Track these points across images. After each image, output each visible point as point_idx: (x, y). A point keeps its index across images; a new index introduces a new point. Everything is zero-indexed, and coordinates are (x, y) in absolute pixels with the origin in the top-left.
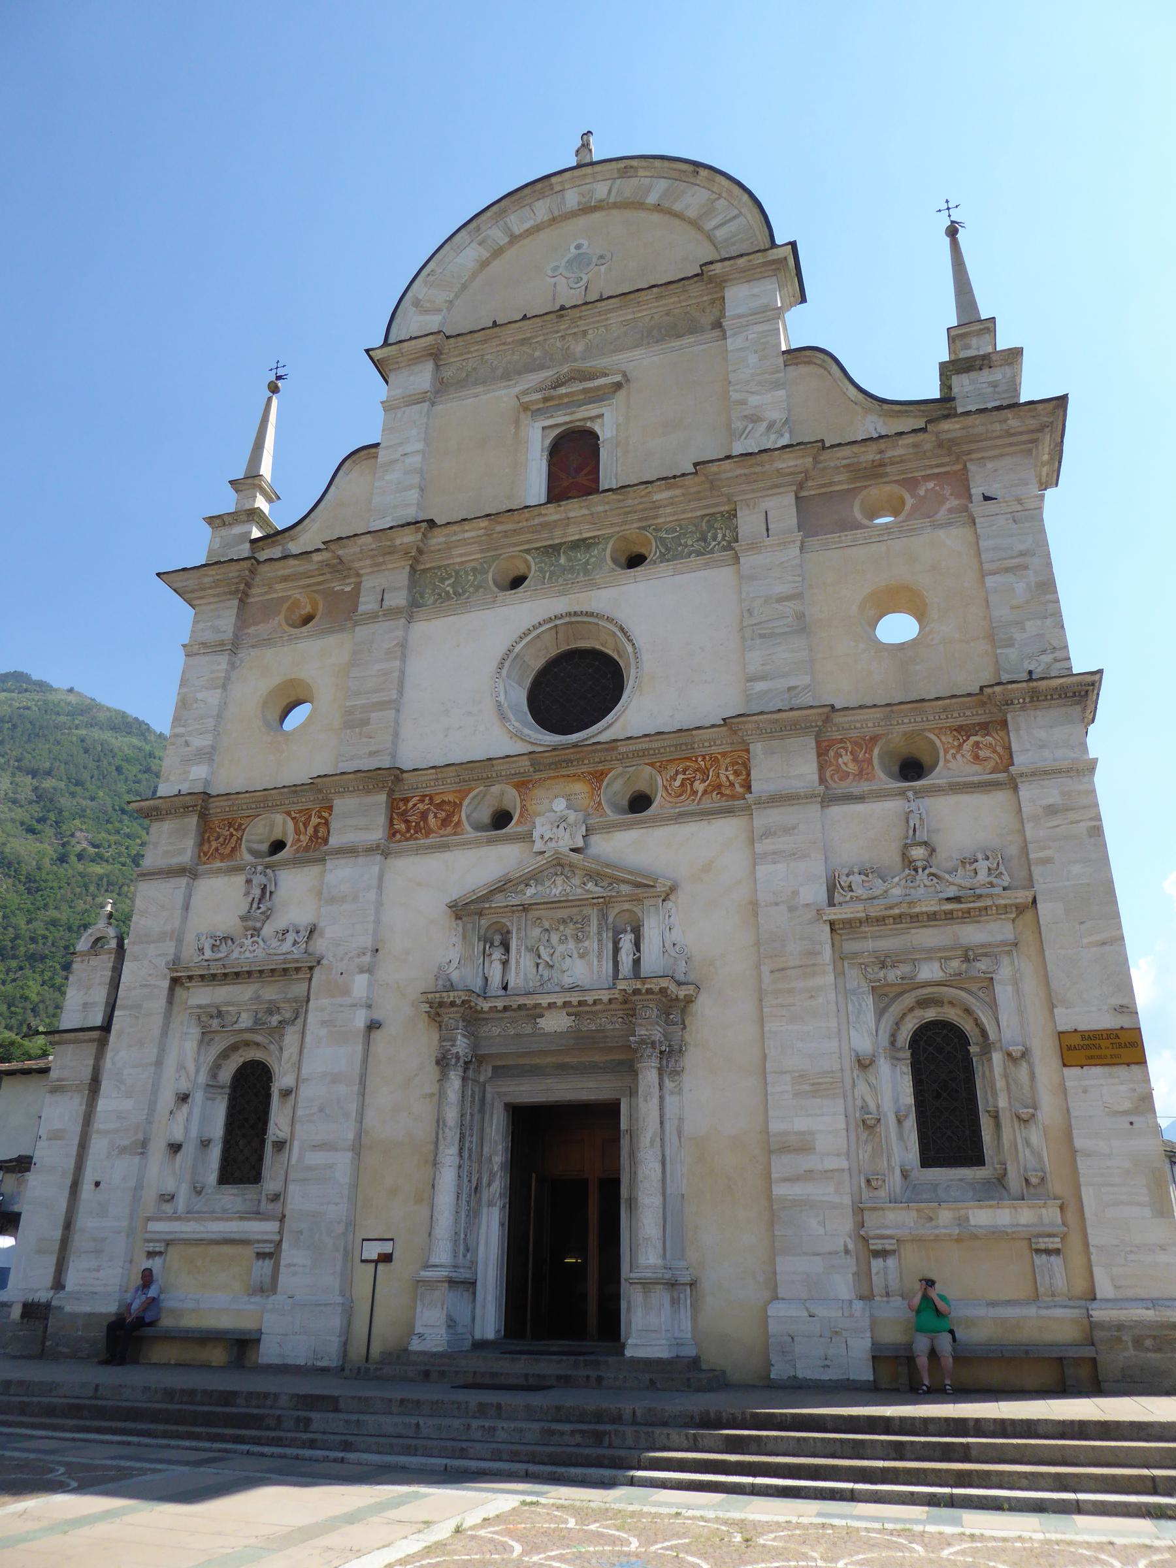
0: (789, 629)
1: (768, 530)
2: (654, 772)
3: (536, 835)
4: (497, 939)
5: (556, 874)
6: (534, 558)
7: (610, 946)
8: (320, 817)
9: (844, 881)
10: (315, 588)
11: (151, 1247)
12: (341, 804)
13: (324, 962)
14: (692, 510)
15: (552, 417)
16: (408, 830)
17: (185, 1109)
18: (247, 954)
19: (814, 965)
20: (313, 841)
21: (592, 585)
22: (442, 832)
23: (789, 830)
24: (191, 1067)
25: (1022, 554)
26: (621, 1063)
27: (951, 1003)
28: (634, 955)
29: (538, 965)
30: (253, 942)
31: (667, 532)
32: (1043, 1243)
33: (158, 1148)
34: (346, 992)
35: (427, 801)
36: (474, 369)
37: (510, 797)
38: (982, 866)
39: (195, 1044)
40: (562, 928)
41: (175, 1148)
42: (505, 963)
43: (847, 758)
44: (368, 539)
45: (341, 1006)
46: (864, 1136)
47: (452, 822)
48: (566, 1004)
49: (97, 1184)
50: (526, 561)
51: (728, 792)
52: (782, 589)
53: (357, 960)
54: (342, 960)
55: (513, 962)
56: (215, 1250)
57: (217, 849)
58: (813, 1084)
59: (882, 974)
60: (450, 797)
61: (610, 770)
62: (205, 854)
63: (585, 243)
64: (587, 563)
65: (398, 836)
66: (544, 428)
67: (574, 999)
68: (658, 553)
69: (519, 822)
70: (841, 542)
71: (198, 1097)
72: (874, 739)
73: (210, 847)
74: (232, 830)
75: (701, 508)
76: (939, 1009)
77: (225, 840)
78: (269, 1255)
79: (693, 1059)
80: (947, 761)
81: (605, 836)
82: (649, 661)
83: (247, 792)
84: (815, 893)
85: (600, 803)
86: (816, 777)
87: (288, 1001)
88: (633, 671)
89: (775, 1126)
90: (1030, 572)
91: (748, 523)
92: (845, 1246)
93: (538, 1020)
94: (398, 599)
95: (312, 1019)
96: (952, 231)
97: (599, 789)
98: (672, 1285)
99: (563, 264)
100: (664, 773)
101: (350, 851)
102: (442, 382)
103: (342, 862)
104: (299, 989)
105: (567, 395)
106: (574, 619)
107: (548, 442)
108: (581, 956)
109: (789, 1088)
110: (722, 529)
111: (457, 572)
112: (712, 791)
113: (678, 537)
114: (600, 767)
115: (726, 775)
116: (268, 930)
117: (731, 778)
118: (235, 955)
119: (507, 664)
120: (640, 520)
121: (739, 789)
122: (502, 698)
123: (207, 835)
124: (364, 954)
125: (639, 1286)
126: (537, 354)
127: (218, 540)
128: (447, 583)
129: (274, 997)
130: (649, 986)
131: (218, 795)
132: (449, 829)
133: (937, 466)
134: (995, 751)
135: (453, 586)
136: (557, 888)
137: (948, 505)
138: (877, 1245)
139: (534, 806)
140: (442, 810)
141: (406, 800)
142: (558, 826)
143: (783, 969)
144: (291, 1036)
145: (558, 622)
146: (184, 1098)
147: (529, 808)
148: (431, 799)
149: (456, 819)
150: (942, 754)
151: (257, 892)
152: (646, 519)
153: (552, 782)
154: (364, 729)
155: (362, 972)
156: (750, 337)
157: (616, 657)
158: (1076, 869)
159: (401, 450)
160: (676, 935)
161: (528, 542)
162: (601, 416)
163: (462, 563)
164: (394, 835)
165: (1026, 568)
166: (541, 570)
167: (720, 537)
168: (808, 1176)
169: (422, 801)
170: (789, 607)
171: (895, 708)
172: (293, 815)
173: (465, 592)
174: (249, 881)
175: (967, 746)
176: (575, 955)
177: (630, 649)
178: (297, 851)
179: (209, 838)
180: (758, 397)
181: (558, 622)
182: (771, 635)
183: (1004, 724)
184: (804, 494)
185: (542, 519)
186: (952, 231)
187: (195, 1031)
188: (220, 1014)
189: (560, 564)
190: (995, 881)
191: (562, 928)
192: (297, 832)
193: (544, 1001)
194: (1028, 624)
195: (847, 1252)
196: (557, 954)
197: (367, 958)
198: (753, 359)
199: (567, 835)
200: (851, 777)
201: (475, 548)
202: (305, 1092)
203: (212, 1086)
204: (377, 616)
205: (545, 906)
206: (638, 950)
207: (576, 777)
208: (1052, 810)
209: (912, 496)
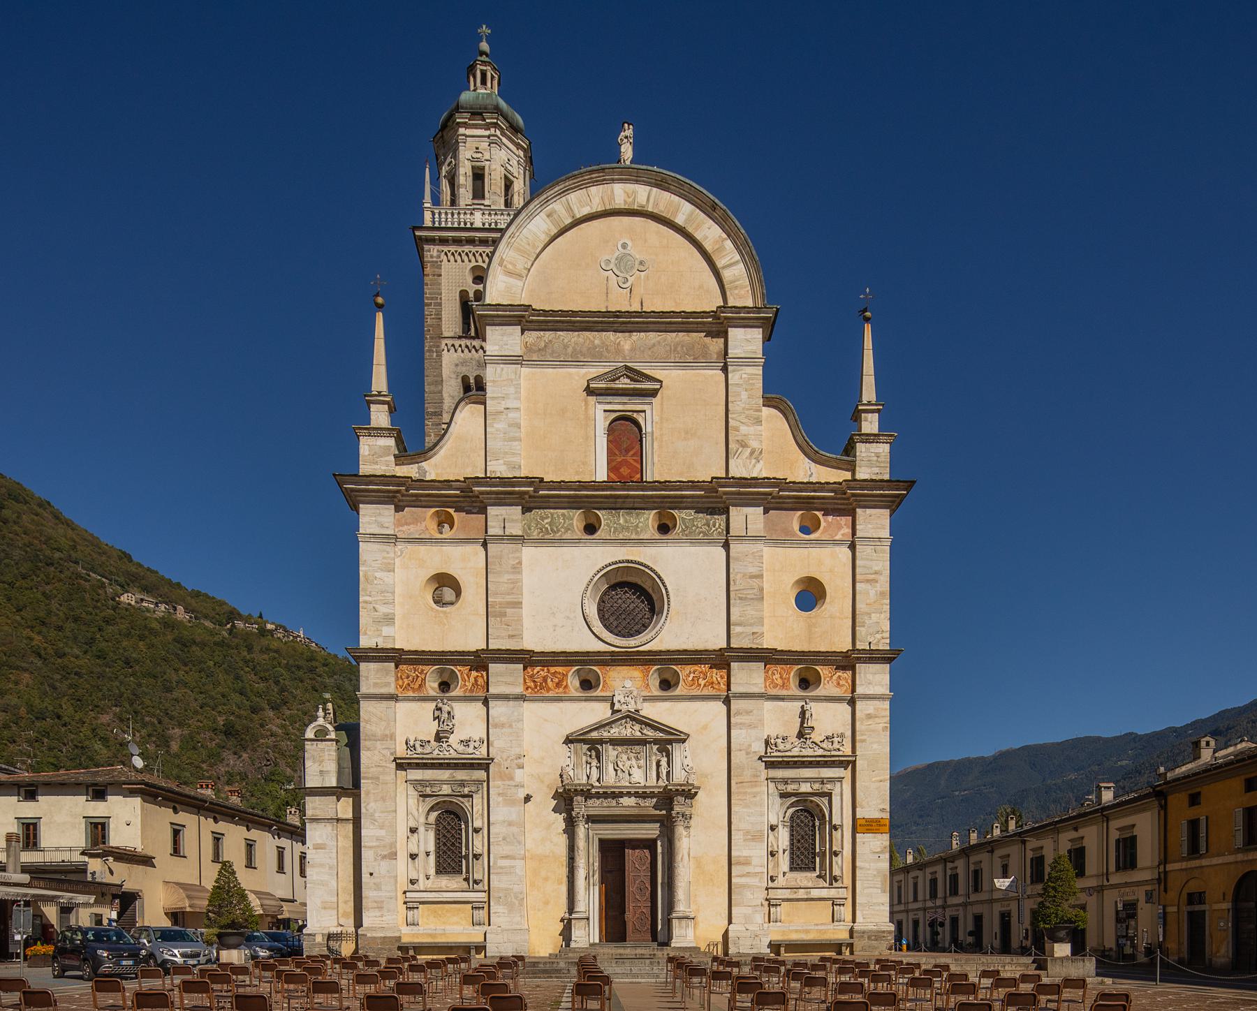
3: (615, 700)
5: (626, 722)
6: (603, 516)
7: (654, 764)
9: (773, 741)
11: (410, 905)
15: (610, 403)
17: (416, 835)
21: (640, 542)
23: (748, 712)
24: (416, 813)
25: (876, 573)
29: (616, 770)
32: (838, 902)
33: (402, 857)
34: (512, 779)
36: (550, 341)
38: (836, 740)
41: (413, 857)
43: (777, 676)
46: (770, 858)
49: (371, 874)
52: (753, 570)
57: (409, 685)
62: (401, 687)
63: (630, 243)
65: (530, 690)
66: (605, 411)
69: (602, 690)
71: (422, 829)
73: (404, 683)
79: (692, 822)
80: (824, 684)
84: (760, 748)
85: (648, 685)
86: (763, 686)
90: (878, 585)
98: (687, 918)
99: (613, 261)
102: (526, 347)
103: (499, 703)
104: (481, 774)
107: (608, 423)
111: (552, 514)
116: (453, 740)
118: (436, 752)
119: (590, 587)
123: (399, 675)
126: (597, 342)
128: (546, 521)
129: (464, 778)
132: (561, 690)
134: (847, 682)
135: (550, 524)
136: (629, 731)
137: (842, 532)
138: (773, 902)
144: (478, 801)
145: (621, 565)
146: (413, 831)
149: (564, 683)
156: (744, 376)
158: (875, 746)
159: (504, 404)
162: (644, 411)
164: (527, 689)
165: (877, 582)
166: (608, 525)
167: (717, 524)
168: (748, 874)
170: (755, 583)
173: (558, 531)
175: (835, 678)
176: (636, 767)
177: (664, 592)
178: (465, 691)
182: (746, 599)
190: (841, 748)
193: (625, 791)
194: (873, 615)
195: (762, 905)
198: (744, 395)
199: (633, 702)
208: (869, 716)
209: (825, 521)
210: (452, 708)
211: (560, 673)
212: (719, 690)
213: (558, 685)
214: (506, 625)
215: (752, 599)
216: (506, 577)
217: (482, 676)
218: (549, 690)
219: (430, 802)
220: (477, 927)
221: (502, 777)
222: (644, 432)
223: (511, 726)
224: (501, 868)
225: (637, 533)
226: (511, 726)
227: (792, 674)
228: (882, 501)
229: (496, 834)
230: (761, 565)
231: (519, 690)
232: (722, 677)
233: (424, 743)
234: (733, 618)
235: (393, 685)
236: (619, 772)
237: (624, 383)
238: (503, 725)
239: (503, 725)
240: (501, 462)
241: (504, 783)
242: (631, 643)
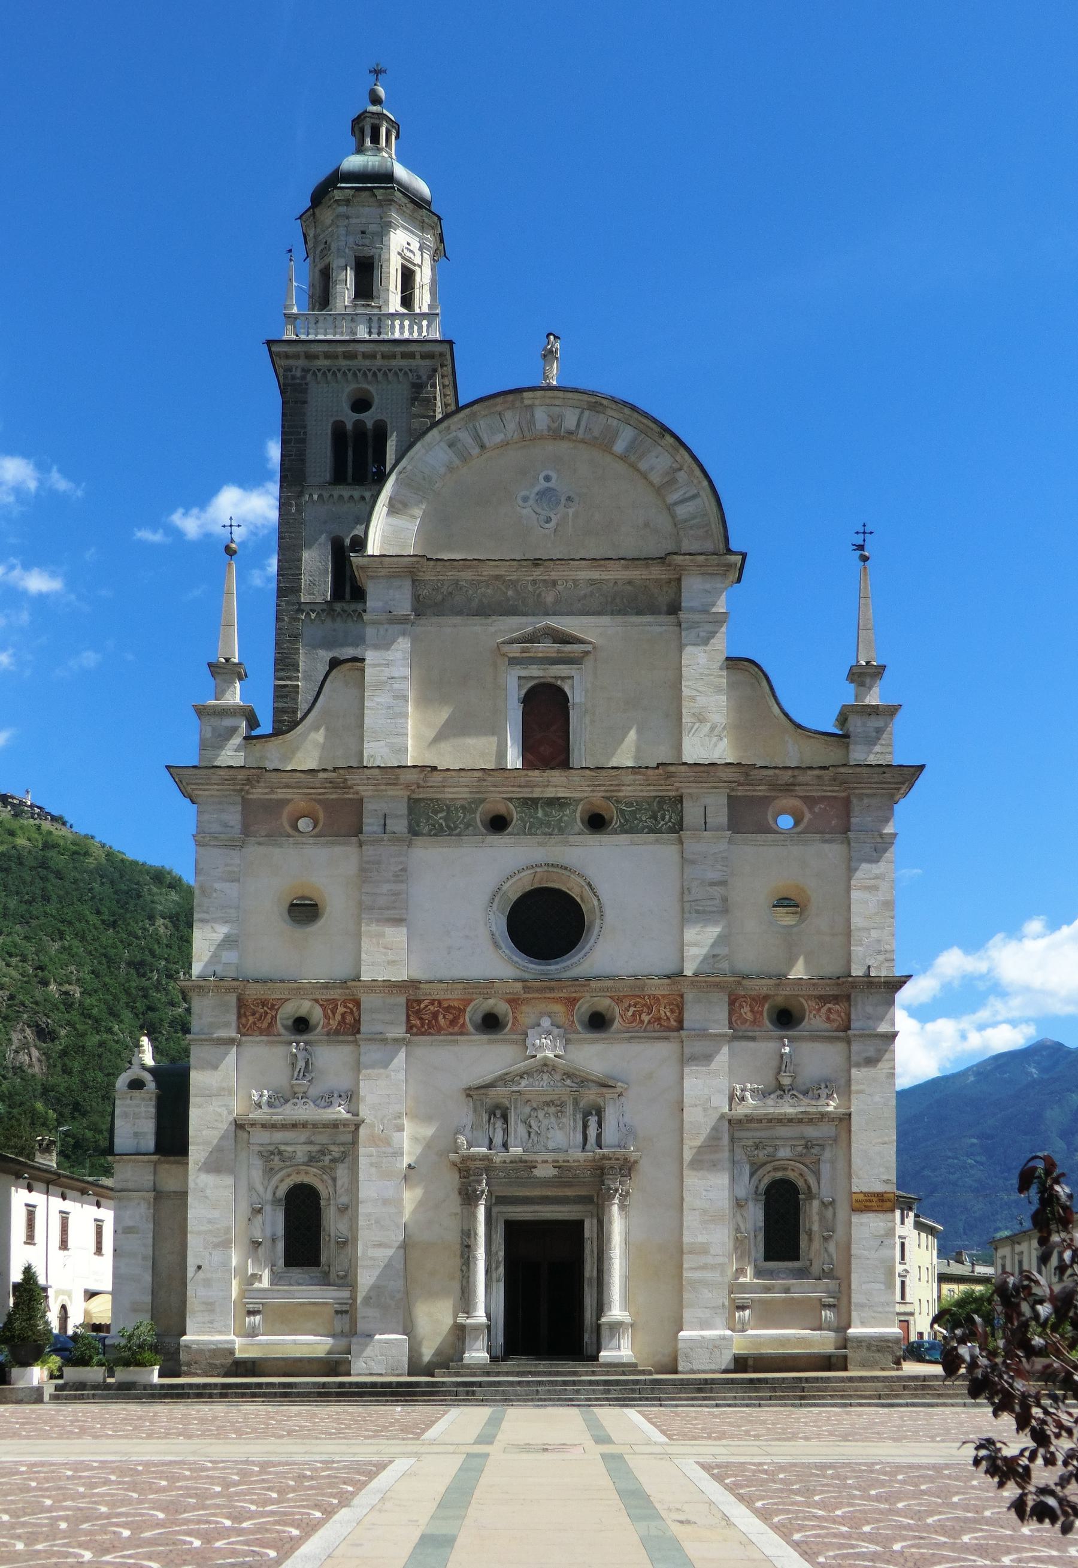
0: (715, 909)
1: (705, 823)
2: (613, 1004)
4: (498, 1113)
10: (314, 796)
14: (648, 791)
16: (423, 1026)
17: (259, 1217)
22: (451, 1030)
24: (260, 1189)
29: (529, 1133)
31: (627, 805)
37: (502, 1008)
39: (261, 1173)
42: (506, 1131)
44: (377, 771)
47: (458, 1023)
48: (554, 1161)
50: (508, 808)
51: (665, 1024)
52: (712, 875)
55: (512, 1129)
57: (254, 1023)
60: (456, 1004)
61: (581, 998)
64: (560, 820)
65: (415, 1030)
67: (561, 1157)
72: (766, 998)
74: (265, 1008)
77: (261, 1016)
82: (610, 915)
85: (573, 1022)
88: (598, 922)
91: (692, 813)
92: (723, 1303)
94: (399, 826)
95: (363, 1161)
97: (573, 1010)
100: (620, 1005)
106: (551, 869)
108: (560, 1129)
110: (668, 811)
111: (448, 807)
112: (654, 1022)
113: (634, 812)
114: (574, 995)
115: (664, 1012)
119: (497, 900)
121: (673, 1023)
122: (494, 929)
127: (209, 729)
128: (440, 815)
132: (456, 1029)
133: (830, 791)
135: (445, 819)
141: (419, 1002)
144: (341, 1171)
149: (461, 1021)
150: (807, 1013)
151: (301, 1064)
157: (578, 900)
163: (452, 799)
166: (521, 819)
167: (667, 817)
169: (433, 1004)
170: (717, 891)
172: (321, 1003)
173: (456, 828)
175: (824, 1010)
176: (556, 1127)
181: (538, 870)
182: (704, 912)
183: (848, 998)
184: (733, 794)
187: (258, 1163)
188: (280, 1153)
191: (546, 1108)
192: (326, 1016)
196: (543, 1126)
200: (748, 1023)
201: (467, 789)
203: (275, 1201)
204: (382, 840)
207: (556, 1000)
210: (310, 1054)
211: (455, 1008)
213: (453, 1022)
215: (714, 912)
216: (385, 888)
217: (352, 1012)
221: (374, 1140)
224: (372, 1258)
227: (766, 1006)
228: (882, 789)
229: (370, 1214)
230: (725, 869)
232: (672, 1011)
235: (234, 1025)
236: (532, 1135)
237: (546, 648)
240: (382, 743)
241: (379, 1149)
242: (553, 968)
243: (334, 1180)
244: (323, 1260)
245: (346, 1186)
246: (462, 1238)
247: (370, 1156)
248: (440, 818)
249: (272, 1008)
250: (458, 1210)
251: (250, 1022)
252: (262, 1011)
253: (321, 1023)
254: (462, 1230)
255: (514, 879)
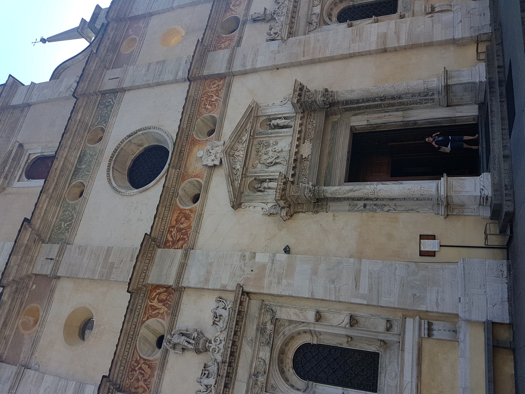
3: (211, 164)
5: (233, 155)
8: (154, 298)
12: (152, 279)
13: (242, 283)
16: (184, 239)
18: (221, 346)
19: (305, 41)
20: (167, 303)
21: (102, 152)
22: (192, 219)
23: (245, 56)
26: (333, 127)
27: (331, 9)
28: (282, 119)
29: (276, 163)
30: (215, 341)
34: (264, 267)
35: (172, 230)
40: (260, 154)
45: (271, 270)
47: (189, 214)
51: (221, 87)
53: (246, 261)
54: (244, 271)
56: (425, 378)
58: (357, 36)
59: (314, 24)
60: (175, 216)
68: (104, 124)
70: (136, 56)
73: (142, 386)
75: (94, 106)
76: (333, 16)
77: (141, 373)
78: (430, 324)
81: (222, 136)
83: (117, 346)
87: (260, 314)
89: (373, 47)
93: (304, 157)
96: (43, 41)
97: (199, 141)
101: (183, 267)
103: (186, 276)
104: (254, 305)
105: (10, 168)
108: (277, 143)
109: (357, 44)
111: (61, 220)
115: (214, 88)
116: (210, 333)
117: (215, 86)
119: (119, 189)
120: (85, 131)
124: (244, 256)
125: (448, 81)
129: (255, 327)
130: (298, 89)
131: (110, 370)
132: (192, 215)
135: (65, 222)
139: (197, 171)
140: (181, 220)
142: (210, 153)
143: (304, 52)
144: (283, 314)
145: (112, 166)
147: (197, 173)
148: (172, 227)
149: (188, 212)
150: (233, 16)
152: (86, 128)
153: (188, 163)
154: (116, 266)
155: (254, 257)
157: (141, 149)
160: (278, 102)
161: (66, 181)
168: (397, 34)
171: (209, 25)
172: (146, 318)
174: (174, 346)
175: (233, 8)
179: (135, 388)
180: (62, 87)
181: (112, 166)
185: (59, 170)
186: (43, 41)
188: (256, 375)
189: (85, 167)
193: (295, 150)
197: (247, 254)
199: (217, 149)
202: (319, 295)
205: (248, 160)
206: (280, 118)
209: (132, 35)
211: (178, 216)
212: (223, 85)
214: (121, 263)
215: (162, 67)
217: (159, 294)
218: (190, 227)
219: (277, 379)
220: (461, 336)
222: (39, 154)
223: (211, 264)
224: (370, 290)
225: (95, 155)
226: (211, 264)
231: (179, 253)
232: (213, 85)
233: (205, 372)
234: (171, 77)
236: (277, 161)
238: (208, 272)
239: (208, 272)
243: (291, 322)
244: (372, 349)
245: (297, 311)
246: (356, 211)
247: (270, 283)
248: (64, 225)
249: (137, 362)
250: (330, 214)
251: (143, 384)
252: (138, 372)
253: (160, 320)
254: (349, 211)
255: (112, 179)
